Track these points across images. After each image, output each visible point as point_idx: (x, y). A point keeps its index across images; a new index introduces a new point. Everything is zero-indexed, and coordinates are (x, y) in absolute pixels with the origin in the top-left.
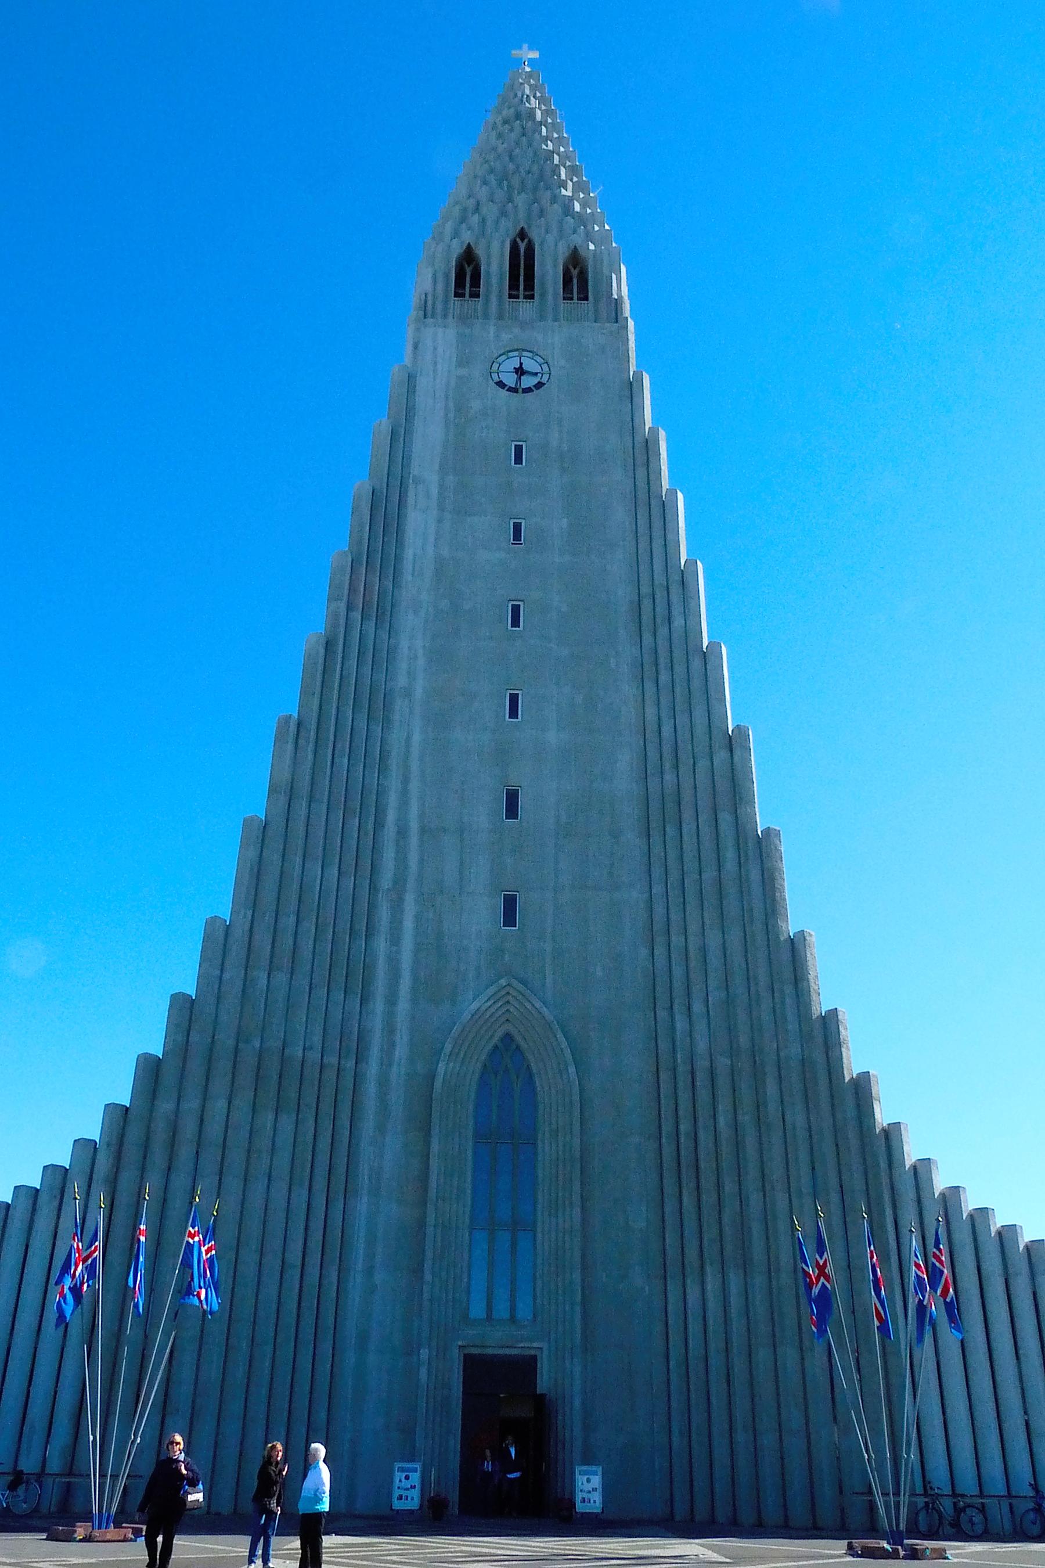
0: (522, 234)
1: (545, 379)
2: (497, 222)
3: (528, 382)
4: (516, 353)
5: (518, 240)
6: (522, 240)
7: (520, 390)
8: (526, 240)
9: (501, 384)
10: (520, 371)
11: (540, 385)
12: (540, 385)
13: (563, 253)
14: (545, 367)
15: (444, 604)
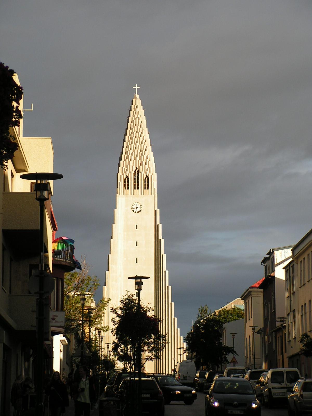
0: (137, 168)
1: (141, 210)
2: (132, 167)
3: (138, 210)
4: (136, 203)
5: (136, 170)
6: (137, 169)
7: (137, 212)
8: (137, 169)
9: (133, 211)
10: (137, 208)
11: (140, 211)
12: (140, 211)
13: (145, 176)
14: (141, 206)
15: (125, 259)
